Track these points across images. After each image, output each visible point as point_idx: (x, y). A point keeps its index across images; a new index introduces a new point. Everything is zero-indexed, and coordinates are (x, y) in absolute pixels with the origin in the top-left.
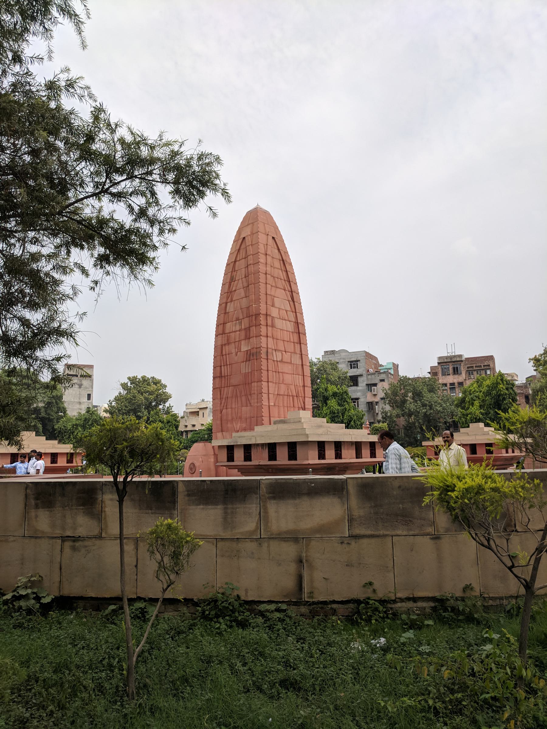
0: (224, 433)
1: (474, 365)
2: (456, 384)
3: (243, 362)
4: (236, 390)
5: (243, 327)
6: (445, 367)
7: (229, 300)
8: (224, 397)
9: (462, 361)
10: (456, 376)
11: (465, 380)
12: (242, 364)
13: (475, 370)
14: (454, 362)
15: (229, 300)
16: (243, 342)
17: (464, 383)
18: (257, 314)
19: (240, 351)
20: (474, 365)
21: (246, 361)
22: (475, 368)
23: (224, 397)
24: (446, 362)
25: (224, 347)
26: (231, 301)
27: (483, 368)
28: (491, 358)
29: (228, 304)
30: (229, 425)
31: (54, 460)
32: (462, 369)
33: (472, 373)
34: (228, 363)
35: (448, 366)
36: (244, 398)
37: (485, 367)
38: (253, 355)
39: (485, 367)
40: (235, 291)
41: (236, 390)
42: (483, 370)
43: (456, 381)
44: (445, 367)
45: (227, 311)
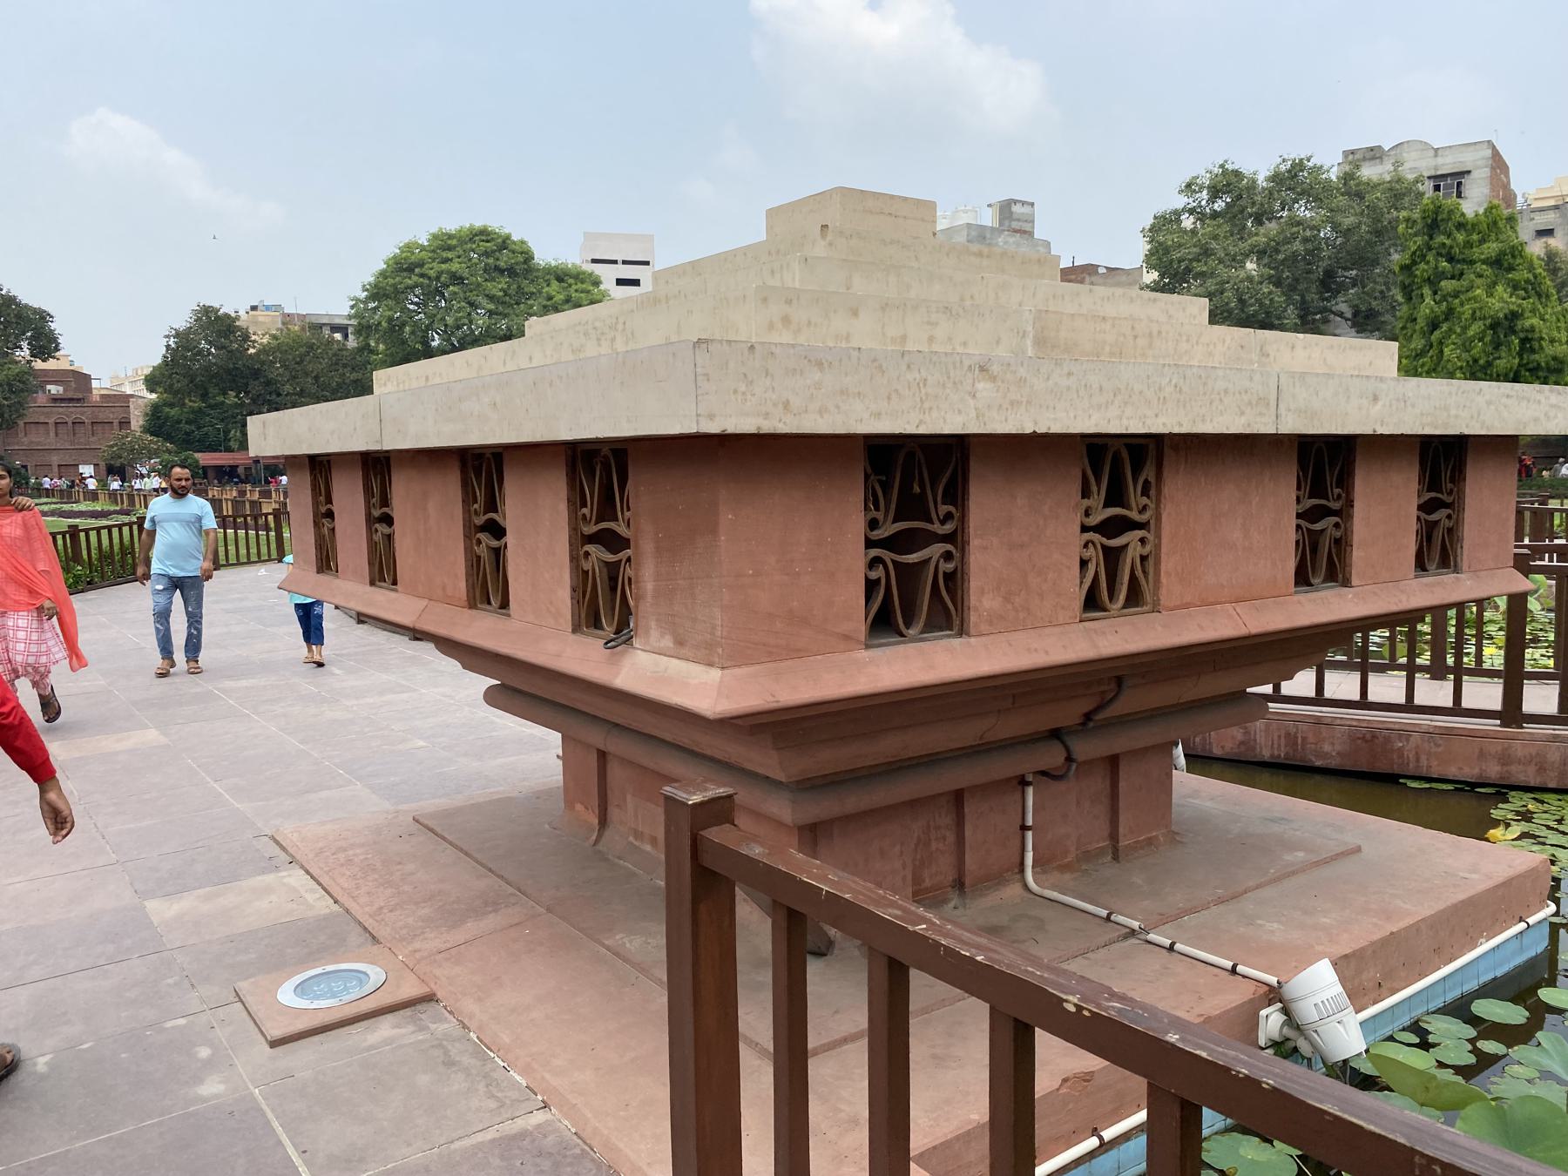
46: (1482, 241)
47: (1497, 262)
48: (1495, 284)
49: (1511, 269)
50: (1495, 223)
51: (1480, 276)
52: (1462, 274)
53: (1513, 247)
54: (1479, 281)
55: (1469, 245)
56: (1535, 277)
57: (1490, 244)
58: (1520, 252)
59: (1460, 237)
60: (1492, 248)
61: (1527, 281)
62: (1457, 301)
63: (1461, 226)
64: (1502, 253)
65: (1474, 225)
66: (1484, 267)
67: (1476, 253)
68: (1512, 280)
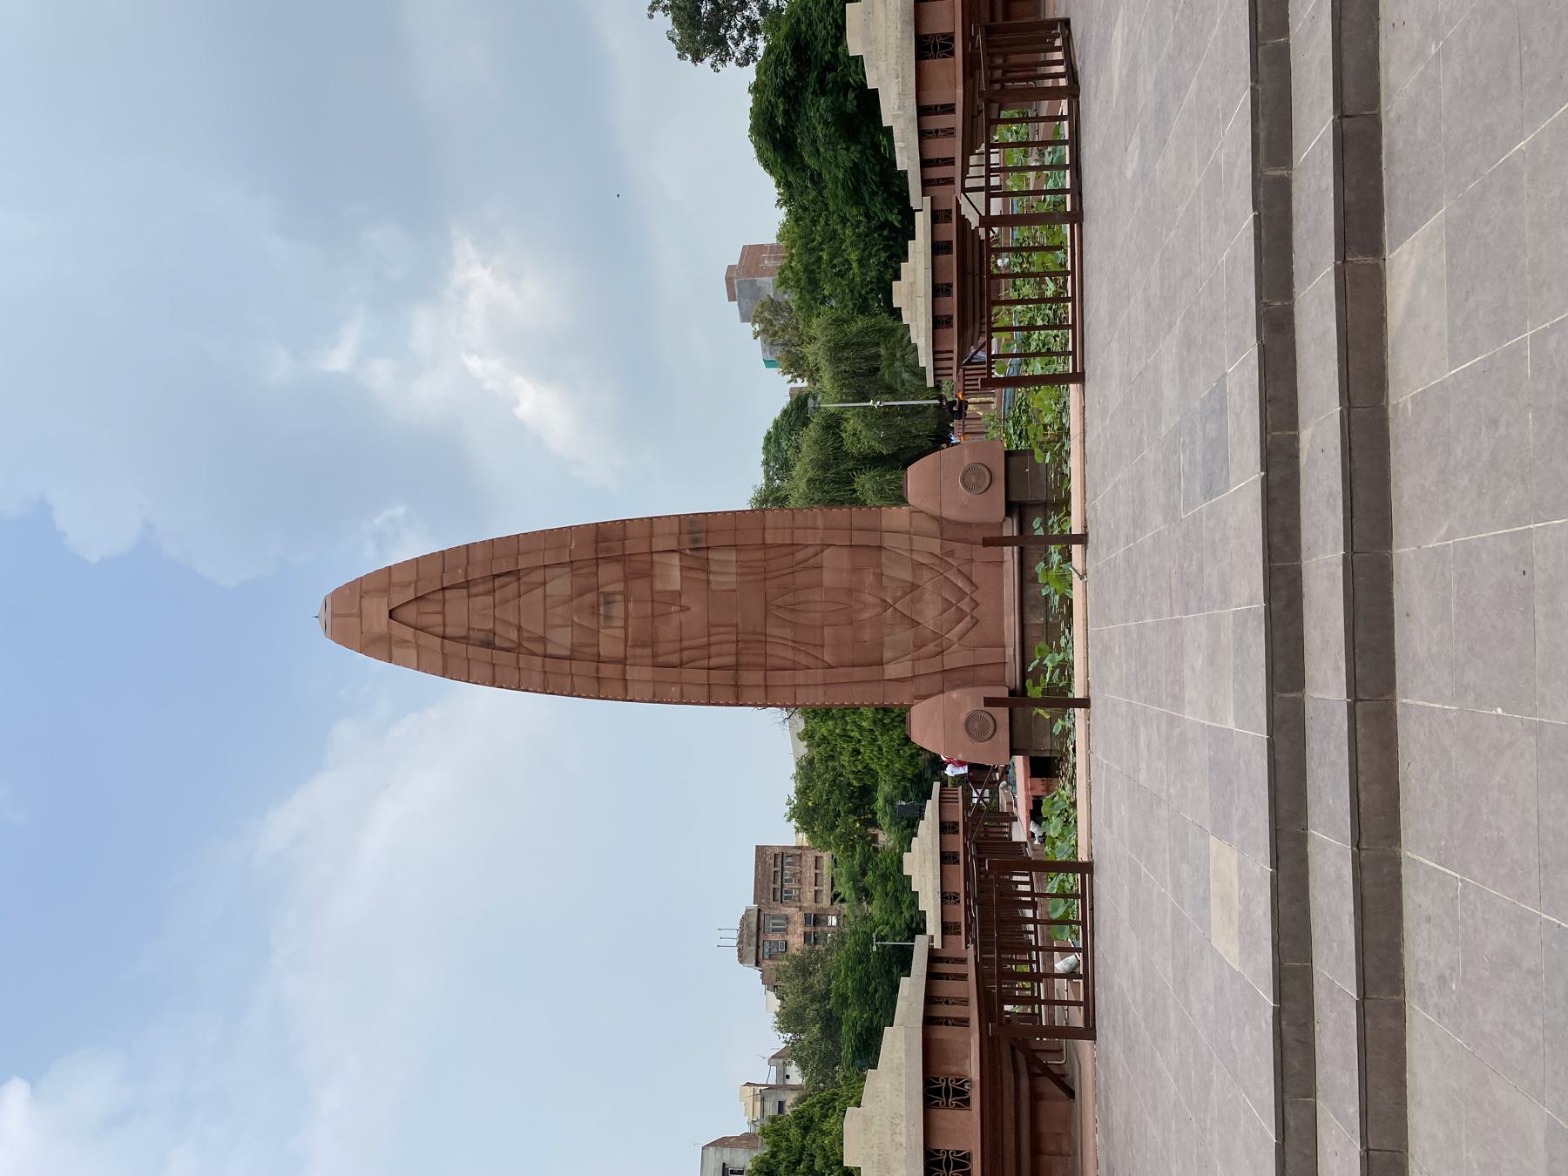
0: (888, 655)
1: (772, 885)
2: (808, 929)
3: (708, 582)
4: (779, 607)
5: (619, 587)
6: (767, 950)
7: (537, 648)
8: (789, 655)
9: (759, 911)
10: (791, 928)
11: (800, 907)
12: (713, 586)
13: (782, 885)
14: (758, 929)
15: (537, 648)
16: (659, 586)
17: (808, 912)
18: (597, 535)
19: (679, 594)
20: (772, 885)
21: (708, 572)
22: (778, 885)
23: (789, 655)
24: (758, 947)
25: (661, 660)
26: (543, 640)
27: (779, 869)
28: (761, 851)
29: (551, 650)
30: (867, 634)
31: (943, 47)
32: (777, 912)
33: (786, 892)
34: (705, 640)
35: (767, 944)
36: (802, 578)
37: (779, 864)
38: (696, 540)
39: (779, 864)
40: (520, 628)
41: (779, 607)
42: (783, 868)
43: (800, 930)
44: (767, 950)
45: (567, 653)
46: (788, 1140)
47: (806, 1130)
48: (821, 1131)
49: (811, 1120)
50: (775, 1131)
51: (814, 1141)
52: (811, 1155)
53: (795, 1117)
54: (819, 1141)
55: (789, 1149)
56: (820, 1102)
57: (791, 1134)
58: (800, 1113)
59: (782, 1156)
60: (794, 1132)
61: (822, 1108)
62: (832, 1157)
63: (774, 1155)
64: (798, 1125)
65: (775, 1146)
66: (807, 1138)
67: (796, 1144)
68: (820, 1119)
